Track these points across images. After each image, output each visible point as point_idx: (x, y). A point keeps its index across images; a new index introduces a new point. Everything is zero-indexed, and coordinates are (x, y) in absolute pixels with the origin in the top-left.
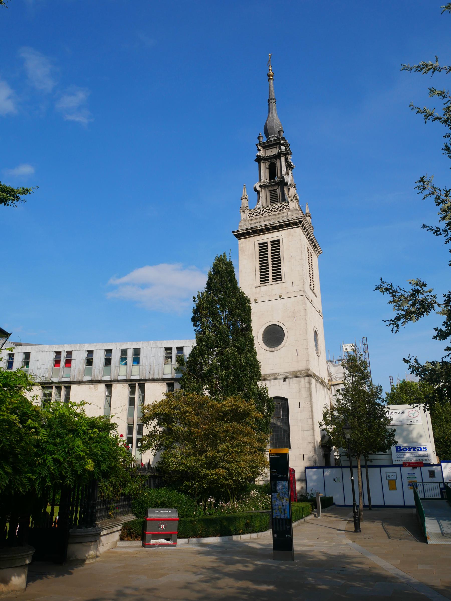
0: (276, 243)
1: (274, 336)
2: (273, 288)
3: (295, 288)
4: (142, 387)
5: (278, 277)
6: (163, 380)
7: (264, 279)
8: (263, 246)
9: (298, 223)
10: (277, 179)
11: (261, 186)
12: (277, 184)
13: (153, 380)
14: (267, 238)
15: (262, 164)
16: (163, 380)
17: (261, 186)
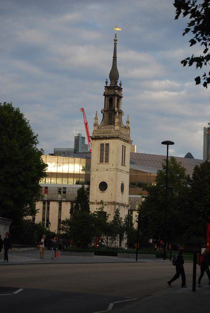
0: (107, 145)
1: (103, 186)
2: (104, 166)
3: (113, 167)
4: (49, 203)
5: (107, 161)
6: (57, 201)
7: (101, 161)
8: (102, 145)
9: (117, 138)
10: (113, 109)
11: (104, 111)
12: (112, 111)
13: (54, 201)
14: (104, 142)
15: (106, 98)
16: (57, 201)
17: (104, 111)
